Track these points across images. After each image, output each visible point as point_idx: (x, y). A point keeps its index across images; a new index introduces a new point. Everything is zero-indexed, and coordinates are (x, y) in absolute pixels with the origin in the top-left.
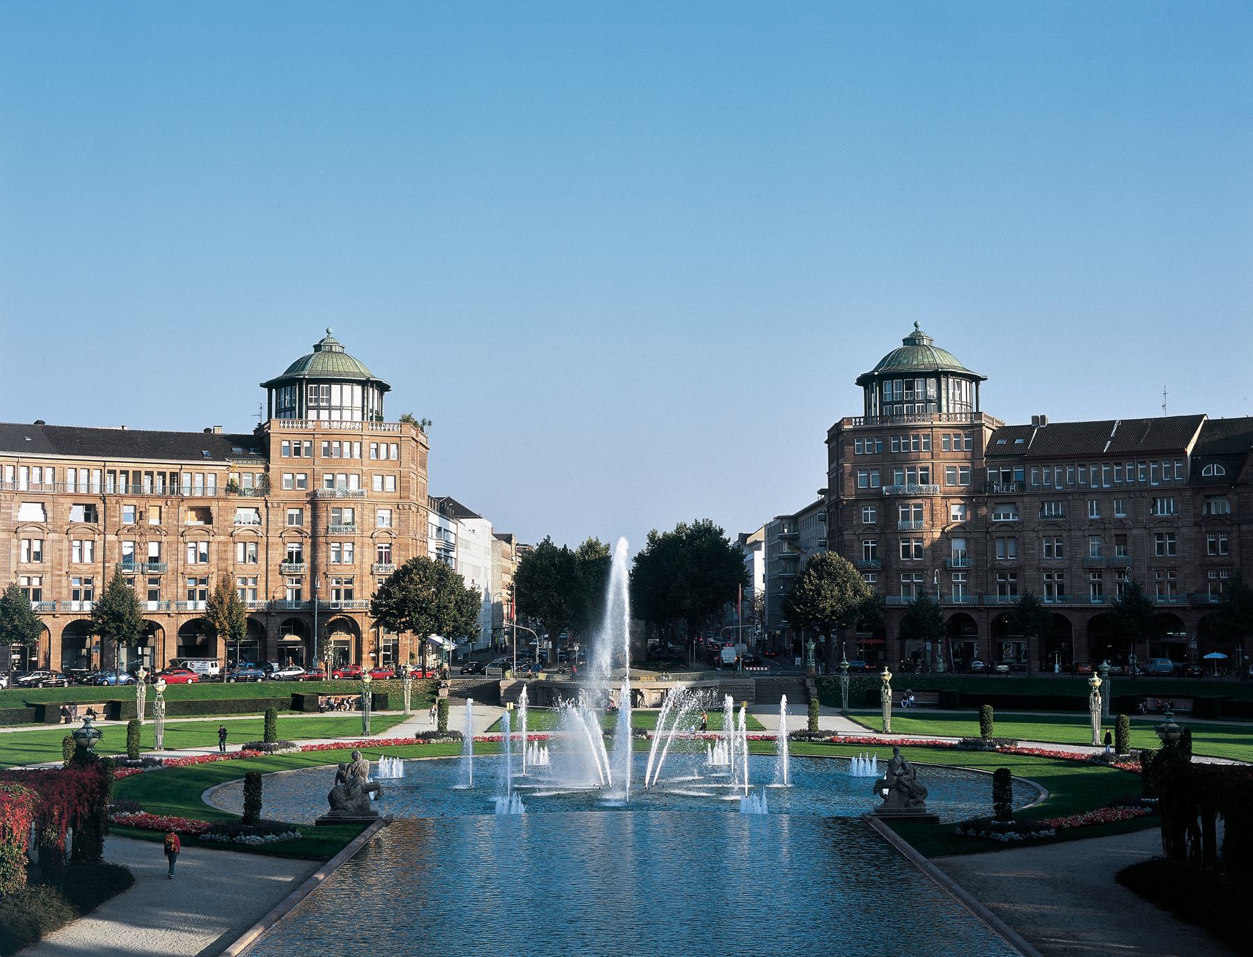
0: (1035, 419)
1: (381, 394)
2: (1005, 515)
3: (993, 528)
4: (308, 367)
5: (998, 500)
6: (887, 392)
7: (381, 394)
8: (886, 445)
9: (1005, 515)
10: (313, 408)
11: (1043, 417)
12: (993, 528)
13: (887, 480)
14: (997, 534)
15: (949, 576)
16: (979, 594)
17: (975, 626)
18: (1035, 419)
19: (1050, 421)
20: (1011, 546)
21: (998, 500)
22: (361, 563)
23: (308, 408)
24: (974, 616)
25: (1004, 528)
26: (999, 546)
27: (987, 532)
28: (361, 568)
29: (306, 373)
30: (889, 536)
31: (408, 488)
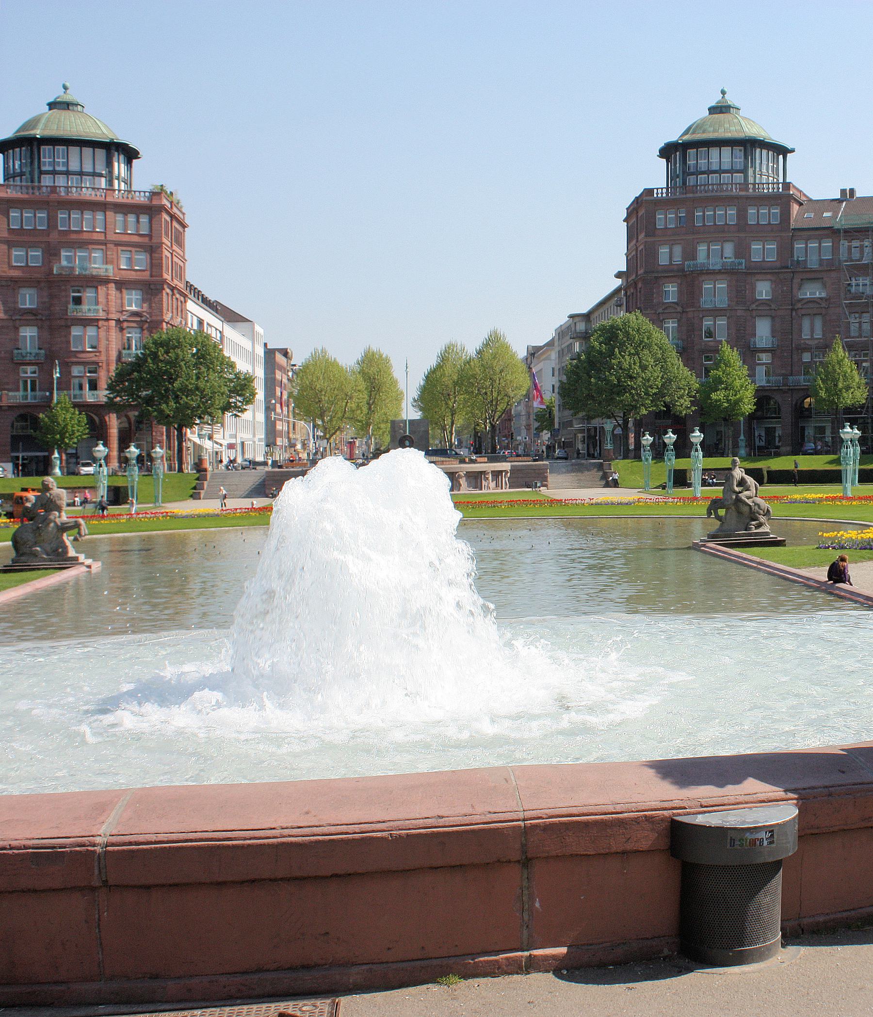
0: (843, 192)
1: (129, 163)
2: (812, 291)
3: (799, 305)
4: (41, 125)
5: (805, 276)
6: (691, 162)
7: (129, 163)
8: (691, 216)
9: (812, 291)
10: (47, 173)
11: (852, 191)
12: (799, 305)
13: (689, 254)
14: (803, 312)
15: (753, 356)
16: (783, 375)
17: (778, 410)
18: (843, 192)
19: (858, 194)
20: (818, 323)
21: (805, 276)
22: (107, 350)
23: (41, 173)
24: (778, 397)
25: (811, 305)
26: (806, 323)
27: (792, 310)
28: (108, 356)
29: (38, 133)
30: (690, 315)
31: (160, 266)
